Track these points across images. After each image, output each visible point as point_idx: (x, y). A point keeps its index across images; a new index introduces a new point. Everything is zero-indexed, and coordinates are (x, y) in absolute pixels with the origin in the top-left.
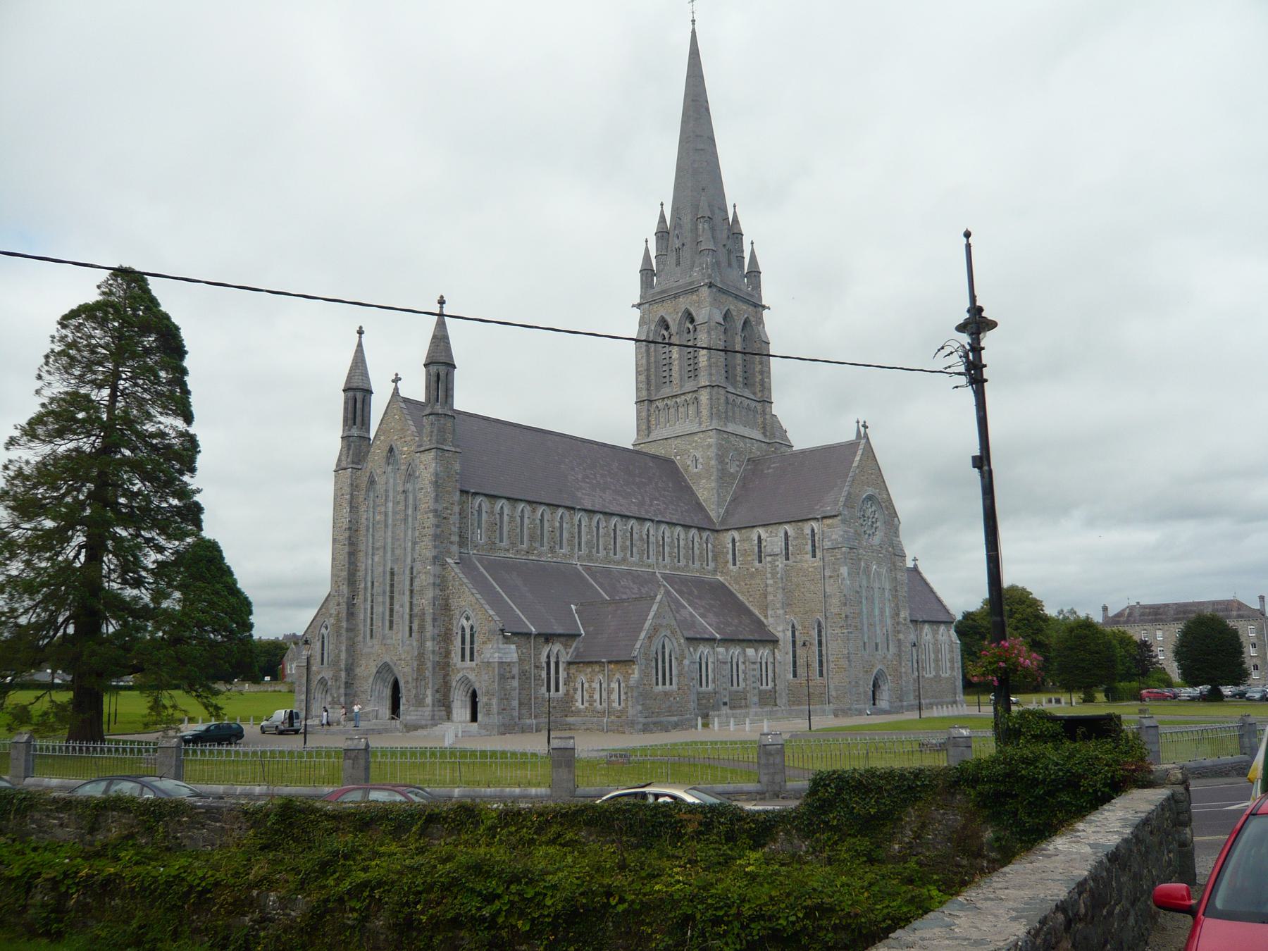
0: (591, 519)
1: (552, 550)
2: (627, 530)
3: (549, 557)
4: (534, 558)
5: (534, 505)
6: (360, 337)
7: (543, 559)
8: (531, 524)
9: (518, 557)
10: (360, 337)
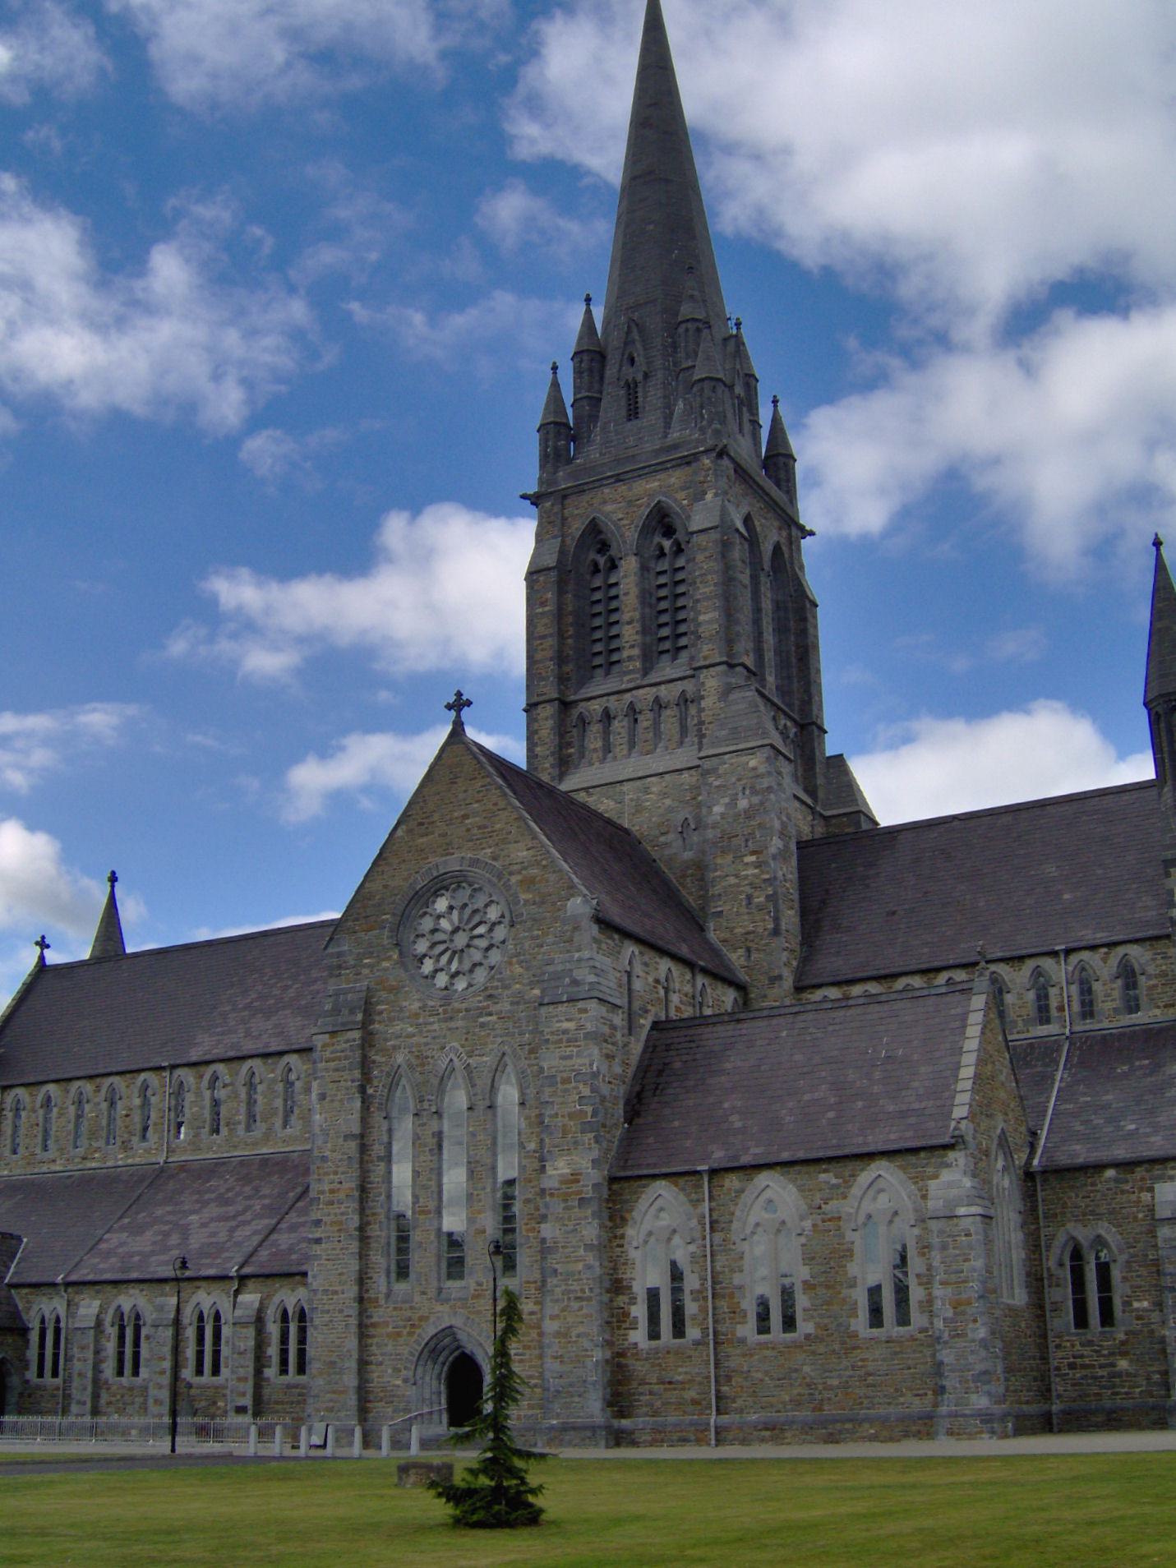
0: (201, 1077)
1: (126, 1146)
2: (274, 1081)
3: (121, 1158)
4: (94, 1165)
5: (98, 1080)
6: (113, 887)
7: (109, 1164)
8: (91, 1112)
9: (69, 1168)
10: (113, 887)
